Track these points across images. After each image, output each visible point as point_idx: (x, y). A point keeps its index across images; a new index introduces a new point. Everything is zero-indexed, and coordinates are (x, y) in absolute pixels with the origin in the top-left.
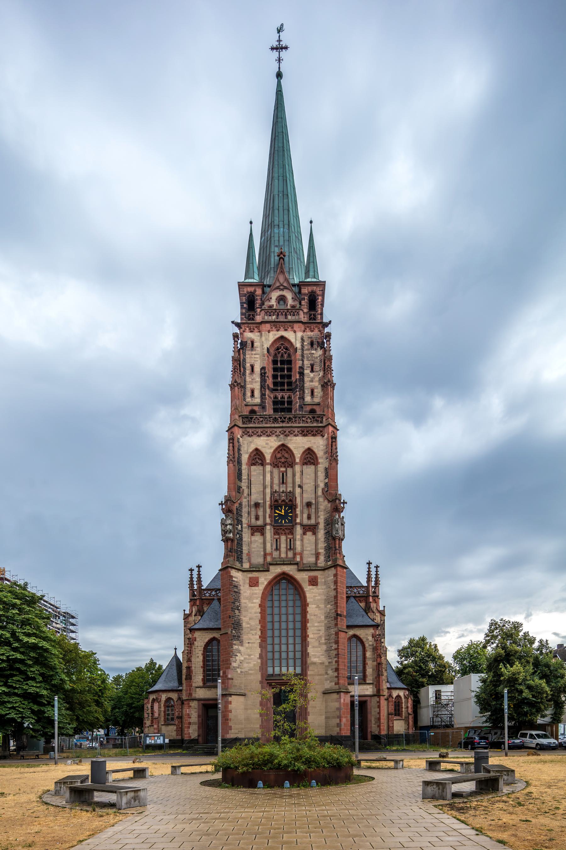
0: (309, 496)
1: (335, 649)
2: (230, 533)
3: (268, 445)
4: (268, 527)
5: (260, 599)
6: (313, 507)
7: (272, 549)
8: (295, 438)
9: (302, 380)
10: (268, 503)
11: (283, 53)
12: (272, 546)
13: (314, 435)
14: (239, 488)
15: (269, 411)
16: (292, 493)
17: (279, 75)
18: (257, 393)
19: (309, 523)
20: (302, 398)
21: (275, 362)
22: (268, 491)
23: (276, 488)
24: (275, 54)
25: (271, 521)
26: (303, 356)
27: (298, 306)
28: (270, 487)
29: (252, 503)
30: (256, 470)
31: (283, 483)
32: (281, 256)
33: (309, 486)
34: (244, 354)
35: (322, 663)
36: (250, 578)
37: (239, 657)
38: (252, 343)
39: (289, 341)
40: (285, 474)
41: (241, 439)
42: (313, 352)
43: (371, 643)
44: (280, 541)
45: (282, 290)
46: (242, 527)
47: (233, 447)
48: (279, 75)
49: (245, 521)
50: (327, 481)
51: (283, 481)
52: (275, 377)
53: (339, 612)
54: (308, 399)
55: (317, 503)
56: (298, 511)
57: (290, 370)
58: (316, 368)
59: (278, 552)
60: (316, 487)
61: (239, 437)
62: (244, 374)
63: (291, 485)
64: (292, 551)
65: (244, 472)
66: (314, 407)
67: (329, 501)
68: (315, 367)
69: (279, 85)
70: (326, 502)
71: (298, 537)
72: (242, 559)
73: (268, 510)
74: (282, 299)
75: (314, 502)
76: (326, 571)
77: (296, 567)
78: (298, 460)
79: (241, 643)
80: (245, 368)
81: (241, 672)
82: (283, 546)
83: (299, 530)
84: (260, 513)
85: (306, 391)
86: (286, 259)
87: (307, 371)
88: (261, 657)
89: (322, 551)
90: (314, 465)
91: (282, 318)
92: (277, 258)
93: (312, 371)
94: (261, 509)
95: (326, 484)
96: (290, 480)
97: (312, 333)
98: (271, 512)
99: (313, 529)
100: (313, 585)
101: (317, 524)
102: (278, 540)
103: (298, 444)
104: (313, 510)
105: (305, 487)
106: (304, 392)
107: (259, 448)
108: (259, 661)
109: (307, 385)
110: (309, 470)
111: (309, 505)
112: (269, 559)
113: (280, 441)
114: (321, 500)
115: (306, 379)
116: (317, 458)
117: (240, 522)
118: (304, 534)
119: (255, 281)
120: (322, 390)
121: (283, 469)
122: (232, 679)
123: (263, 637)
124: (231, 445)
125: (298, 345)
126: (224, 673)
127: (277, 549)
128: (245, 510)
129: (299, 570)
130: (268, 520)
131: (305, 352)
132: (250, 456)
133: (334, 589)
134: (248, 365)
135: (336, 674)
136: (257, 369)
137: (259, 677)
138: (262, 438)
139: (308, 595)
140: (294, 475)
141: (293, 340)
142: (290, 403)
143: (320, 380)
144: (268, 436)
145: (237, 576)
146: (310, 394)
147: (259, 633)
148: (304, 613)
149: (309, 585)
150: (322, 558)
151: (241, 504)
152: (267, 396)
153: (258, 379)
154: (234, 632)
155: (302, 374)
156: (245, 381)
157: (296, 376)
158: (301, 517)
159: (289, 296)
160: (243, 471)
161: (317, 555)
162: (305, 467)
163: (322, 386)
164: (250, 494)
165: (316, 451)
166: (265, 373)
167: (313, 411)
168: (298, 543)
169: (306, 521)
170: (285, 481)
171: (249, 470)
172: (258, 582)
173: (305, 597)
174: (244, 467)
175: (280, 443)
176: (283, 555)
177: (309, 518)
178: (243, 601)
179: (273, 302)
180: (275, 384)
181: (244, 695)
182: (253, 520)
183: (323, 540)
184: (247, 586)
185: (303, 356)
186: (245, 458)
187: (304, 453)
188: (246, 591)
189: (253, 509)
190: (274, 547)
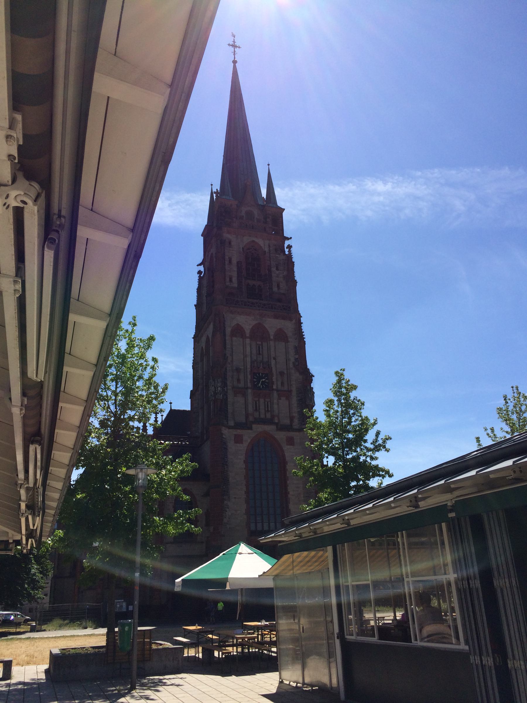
4: (250, 391)
10: (249, 370)
11: (237, 50)
17: (235, 62)
18: (235, 280)
22: (249, 359)
24: (232, 49)
29: (234, 368)
31: (259, 354)
36: (235, 435)
48: (235, 62)
49: (229, 383)
50: (297, 356)
54: (275, 289)
56: (274, 379)
60: (287, 360)
64: (270, 413)
65: (228, 342)
71: (275, 401)
78: (272, 337)
82: (262, 407)
84: (242, 377)
87: (274, 269)
93: (277, 269)
95: (296, 359)
100: (291, 445)
101: (290, 391)
111: (282, 374)
112: (251, 419)
115: (273, 275)
118: (279, 398)
125: (267, 250)
130: (249, 385)
134: (227, 257)
136: (234, 261)
149: (287, 445)
153: (235, 269)
155: (270, 271)
161: (292, 419)
164: (232, 361)
168: (275, 406)
169: (280, 387)
170: (261, 352)
174: (227, 338)
175: (257, 322)
176: (262, 416)
177: (282, 384)
188: (232, 447)
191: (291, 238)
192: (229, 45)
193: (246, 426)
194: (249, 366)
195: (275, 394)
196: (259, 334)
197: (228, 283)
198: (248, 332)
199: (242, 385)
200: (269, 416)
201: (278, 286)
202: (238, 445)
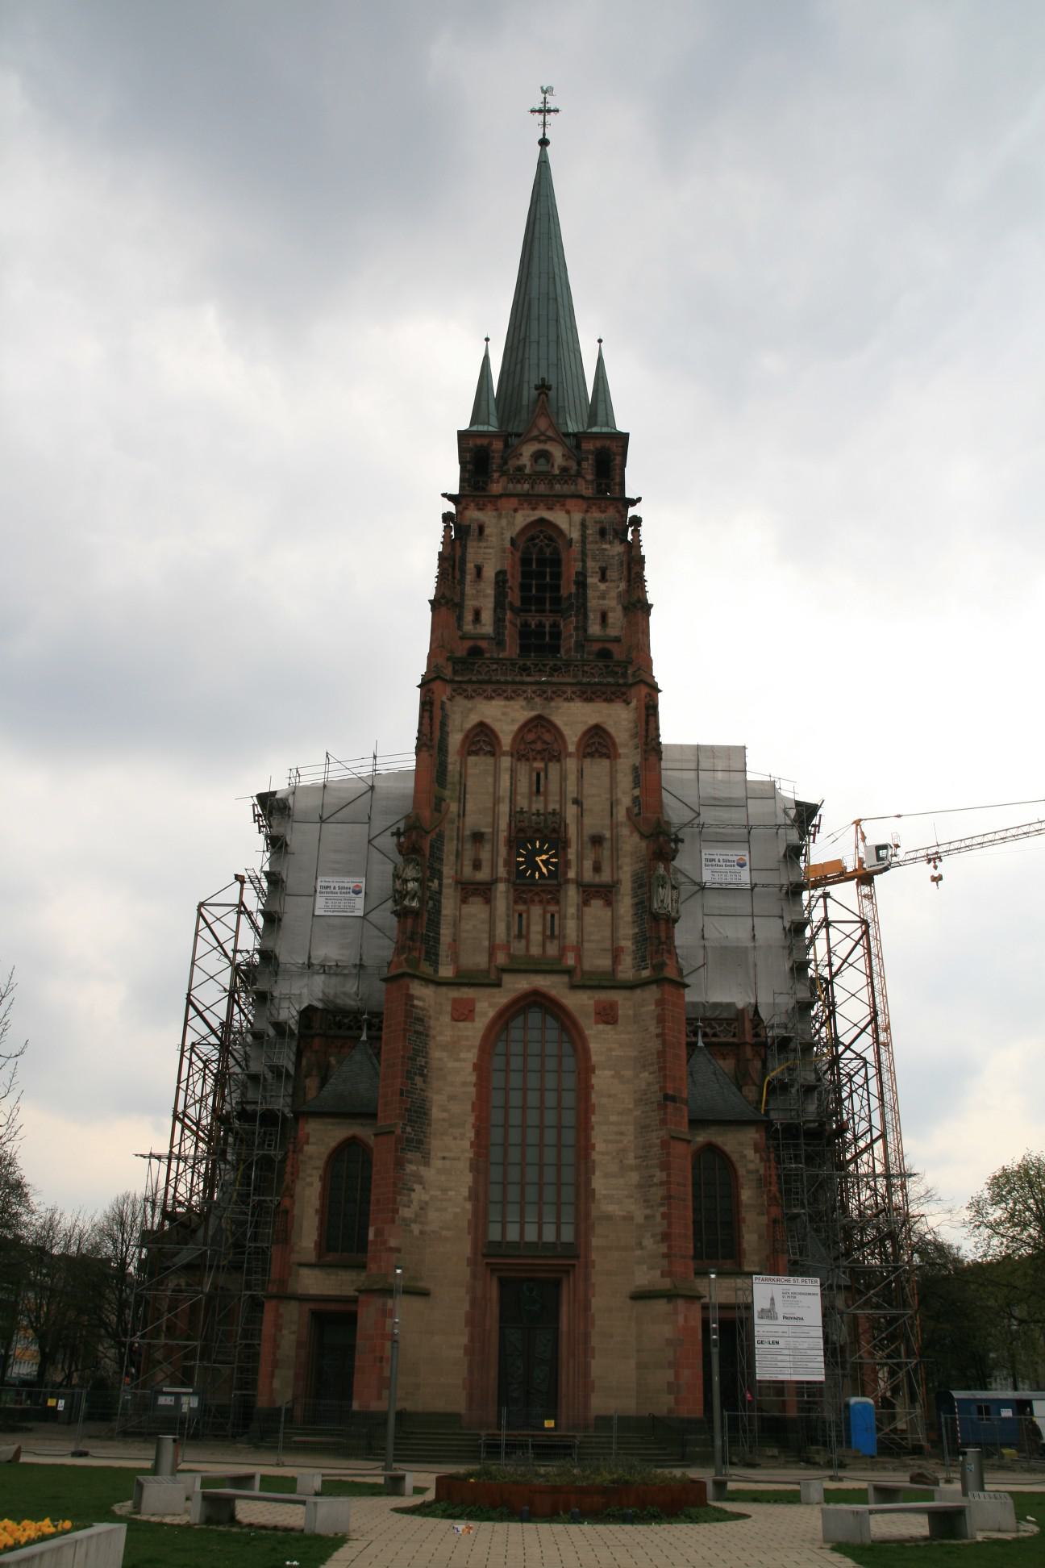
0: (596, 822)
1: (662, 1184)
2: (413, 899)
3: (506, 716)
4: (501, 887)
5: (475, 1051)
6: (607, 845)
7: (508, 935)
8: (566, 704)
10: (503, 835)
11: (550, 117)
12: (508, 928)
13: (609, 700)
14: (440, 800)
15: (511, 650)
16: (558, 815)
17: (544, 142)
18: (487, 617)
19: (597, 879)
20: (583, 627)
21: (525, 561)
22: (504, 808)
23: (522, 803)
24: (539, 117)
25: (509, 872)
26: (584, 553)
27: (575, 467)
29: (468, 833)
30: (478, 766)
32: (543, 388)
33: (596, 802)
34: (464, 547)
35: (629, 1218)
36: (455, 1001)
37: (419, 1195)
38: (481, 529)
40: (542, 775)
41: (448, 704)
43: (751, 1166)
44: (528, 918)
45: (545, 442)
46: (440, 885)
47: (431, 719)
48: (544, 142)
49: (448, 871)
50: (637, 792)
51: (538, 790)
52: (525, 587)
53: (670, 1092)
54: (595, 629)
55: (615, 839)
56: (572, 854)
57: (557, 576)
58: (612, 574)
59: (523, 942)
60: (613, 804)
61: (444, 698)
62: (462, 582)
63: (557, 798)
64: (556, 942)
66: (608, 646)
67: (643, 836)
68: (608, 573)
69: (543, 165)
70: (636, 838)
71: (572, 910)
72: (437, 955)
73: (503, 851)
74: (542, 455)
75: (608, 835)
76: (638, 992)
77: (565, 979)
78: (571, 748)
79: (426, 1161)
80: (463, 572)
81: (421, 1232)
82: (536, 929)
83: (572, 894)
84: (485, 855)
85: (591, 616)
86: (552, 394)
87: (592, 580)
88: (474, 1195)
89: (627, 944)
90: (608, 757)
91: (545, 487)
92: (534, 393)
93: (603, 579)
94: (488, 847)
95: (636, 800)
96: (554, 787)
97: (603, 516)
98: (509, 854)
99: (606, 892)
100: (607, 1023)
102: (524, 916)
103: (574, 718)
104: (607, 853)
105: (587, 804)
106: (586, 616)
107: (488, 721)
108: (468, 1206)
109: (593, 603)
110: (597, 769)
111: (597, 840)
113: (532, 709)
114: (625, 831)
115: (590, 593)
116: (614, 744)
117: (438, 874)
118: (586, 903)
119: (491, 429)
120: (625, 615)
121: (538, 765)
122: (398, 1250)
123: (481, 1145)
124: (427, 714)
125: (575, 535)
126: (379, 1233)
127: (520, 936)
128: (449, 848)
129: (574, 987)
130: (502, 871)
131: (588, 547)
132: (467, 737)
133: (658, 1036)
134: (470, 566)
135: (663, 1248)
137: (466, 1248)
138: (494, 702)
139: (593, 1046)
140: (563, 778)
141: (564, 526)
142: (556, 635)
143: (619, 595)
144: (507, 699)
145: (424, 995)
146: (599, 621)
147: (471, 1134)
148: (584, 1089)
149: (597, 1023)
150: (627, 961)
151: (441, 836)
152: (507, 623)
153: (490, 591)
154: (409, 1129)
155: (582, 584)
156: (463, 594)
157: (568, 588)
158: (579, 865)
159: (557, 452)
160: (450, 767)
161: (616, 954)
162: (587, 762)
163: (625, 609)
164: (462, 814)
165: (612, 730)
166: (505, 582)
167: (605, 654)
168: (571, 925)
169: (588, 876)
171: (463, 764)
172: (472, 1011)
173: (586, 1051)
174: (453, 758)
175: (533, 714)
176: (535, 950)
177: (597, 868)
178: (436, 1054)
179: (525, 459)
180: (525, 600)
181: (424, 1293)
182: (468, 870)
183: (628, 918)
184: (447, 1019)
185: (584, 553)
186: (455, 740)
187: (585, 733)
188: (443, 1029)
189: (468, 846)
190: (515, 930)
191: (639, 499)
192: (532, 111)
193: (488, 980)
194: (503, 823)
195: (572, 894)
197: (468, 627)
198: (506, 741)
199: (483, 875)
200: (552, 949)
201: (604, 617)
202: (461, 1024)
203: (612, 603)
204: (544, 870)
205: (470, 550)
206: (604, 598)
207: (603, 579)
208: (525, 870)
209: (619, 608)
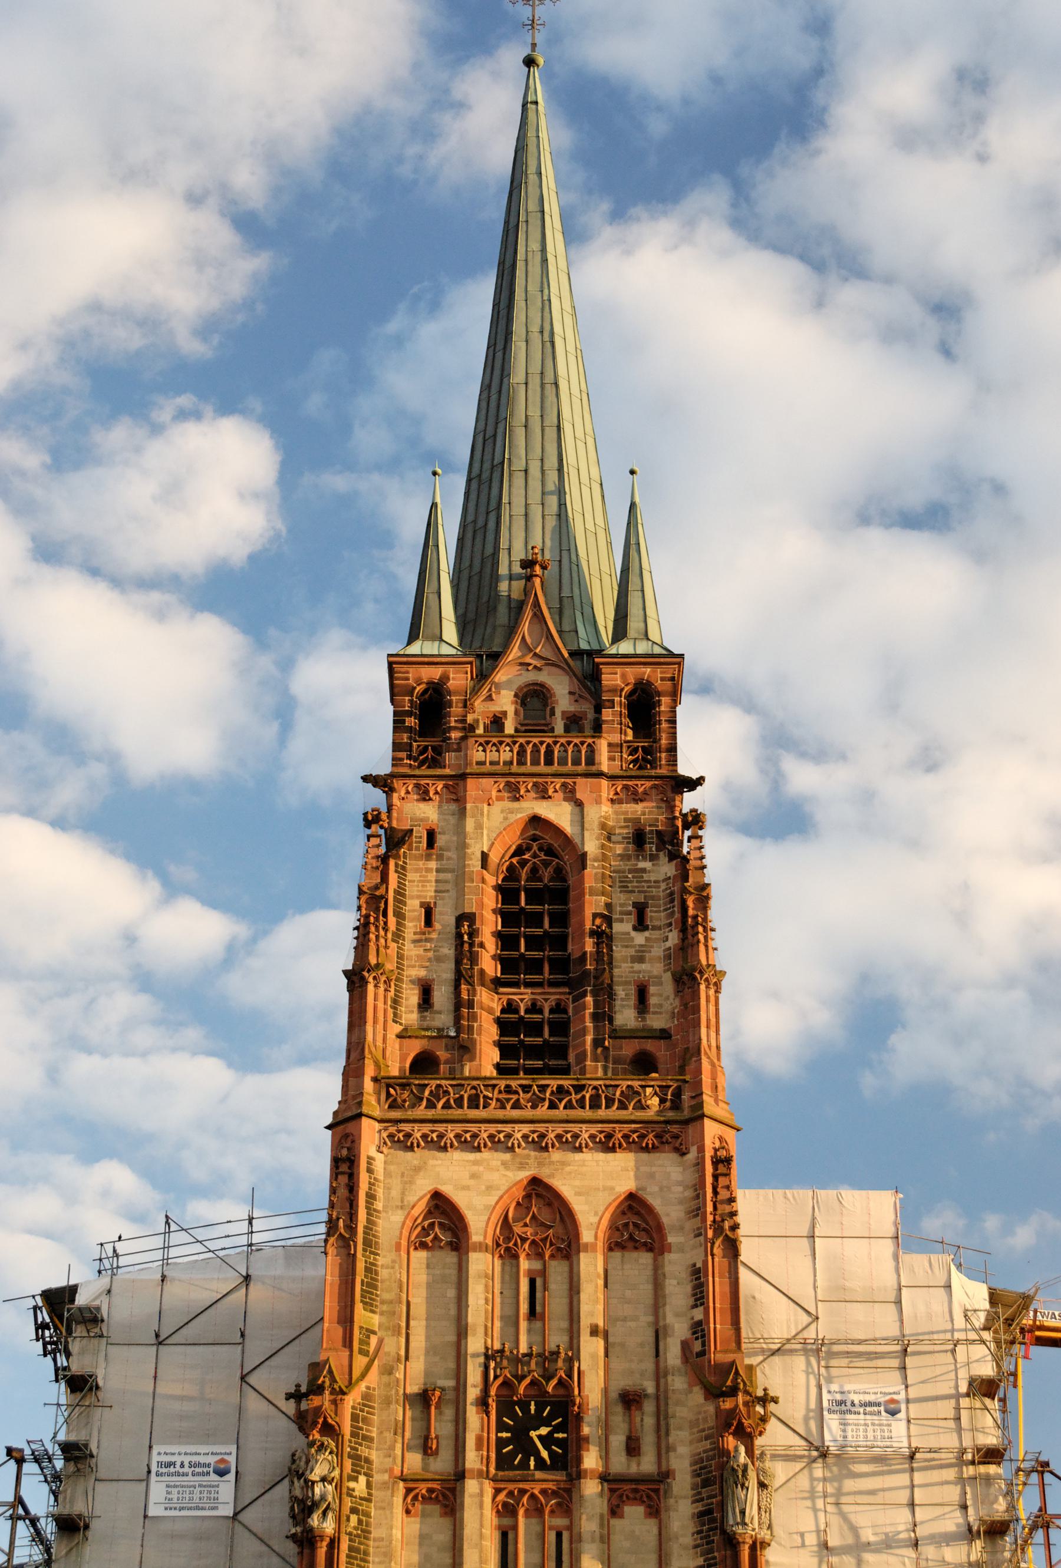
6: (649, 1407)
9: (604, 958)
15: (487, 1057)
19: (634, 1469)
27: (591, 715)
28: (481, 1331)
38: (431, 835)
39: (558, 831)
40: (539, 1282)
42: (642, 865)
50: (698, 1314)
52: (506, 940)
54: (626, 1016)
55: (661, 1398)
57: (561, 919)
58: (655, 916)
60: (659, 1335)
63: (565, 1324)
66: (650, 1046)
68: (649, 913)
70: (698, 1396)
75: (651, 1389)
85: (620, 992)
87: (623, 927)
90: (650, 1250)
93: (641, 925)
104: (649, 1421)
106: (611, 995)
107: (447, 1189)
109: (624, 970)
111: (630, 1400)
113: (522, 1166)
114: (678, 1383)
116: (660, 1228)
119: (446, 650)
120: (678, 992)
124: (343, 1179)
140: (574, 1289)
142: (561, 1027)
143: (668, 957)
146: (633, 1001)
165: (656, 1202)
169: (620, 1463)
170: (538, 1309)
175: (524, 1175)
177: (633, 1448)
180: (507, 964)
191: (700, 781)
196: (542, 1220)
203: (655, 968)
204: (545, 1454)
205: (410, 876)
206: (641, 959)
207: (641, 925)
208: (512, 1455)
209: (668, 977)
